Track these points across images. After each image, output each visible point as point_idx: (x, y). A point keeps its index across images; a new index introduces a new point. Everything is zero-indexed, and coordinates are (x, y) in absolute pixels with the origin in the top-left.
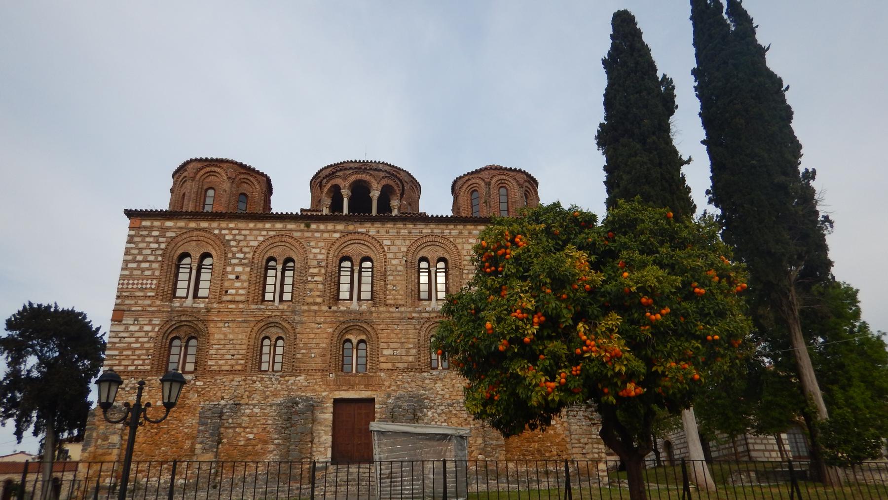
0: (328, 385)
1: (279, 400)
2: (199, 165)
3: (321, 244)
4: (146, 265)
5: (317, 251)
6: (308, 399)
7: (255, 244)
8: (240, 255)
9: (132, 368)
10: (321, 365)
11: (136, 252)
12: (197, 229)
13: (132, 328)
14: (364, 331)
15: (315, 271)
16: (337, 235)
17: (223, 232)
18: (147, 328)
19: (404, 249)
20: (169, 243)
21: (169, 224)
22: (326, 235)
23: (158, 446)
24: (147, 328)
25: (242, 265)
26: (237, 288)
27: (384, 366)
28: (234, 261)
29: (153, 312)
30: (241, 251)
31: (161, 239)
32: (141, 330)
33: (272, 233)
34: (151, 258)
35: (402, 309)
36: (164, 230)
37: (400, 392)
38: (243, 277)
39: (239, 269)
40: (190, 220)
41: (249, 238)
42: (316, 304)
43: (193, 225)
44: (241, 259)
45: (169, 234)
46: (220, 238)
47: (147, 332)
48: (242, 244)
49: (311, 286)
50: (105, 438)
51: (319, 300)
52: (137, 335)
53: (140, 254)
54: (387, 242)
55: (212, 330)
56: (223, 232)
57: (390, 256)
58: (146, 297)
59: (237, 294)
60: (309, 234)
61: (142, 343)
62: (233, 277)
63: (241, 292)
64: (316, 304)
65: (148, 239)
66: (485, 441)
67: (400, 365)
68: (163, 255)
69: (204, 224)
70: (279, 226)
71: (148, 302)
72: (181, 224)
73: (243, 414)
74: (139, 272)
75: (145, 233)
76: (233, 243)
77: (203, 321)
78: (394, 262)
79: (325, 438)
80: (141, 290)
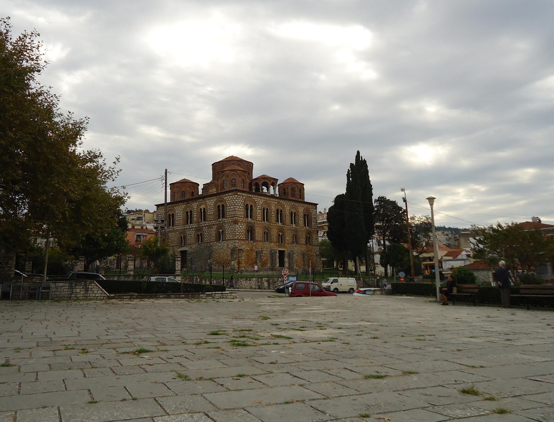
0: (277, 246)
1: (269, 250)
2: (242, 172)
3: (274, 205)
4: (240, 207)
5: (273, 207)
6: (274, 250)
7: (261, 203)
8: (259, 207)
9: (242, 238)
10: (276, 241)
11: (238, 202)
12: (249, 197)
13: (241, 227)
14: (282, 232)
15: (273, 213)
16: (276, 203)
17: (255, 198)
18: (243, 227)
19: (289, 209)
20: (244, 201)
21: (244, 194)
22: (274, 202)
23: (249, 260)
24: (243, 227)
25: (259, 210)
26: (259, 217)
27: (287, 242)
28: (258, 208)
29: (244, 222)
30: (259, 205)
31: (243, 199)
32: (242, 227)
33: (264, 200)
34: (241, 205)
35: (289, 226)
36: (243, 196)
37: (290, 249)
38: (260, 213)
39: (259, 211)
40: (248, 194)
41: (260, 201)
42: (274, 223)
43: (248, 195)
44: (259, 208)
45: (244, 198)
46: (254, 200)
47: (243, 228)
48: (259, 203)
49: (273, 218)
50: (241, 258)
51: (274, 222)
52: (242, 228)
53: (239, 203)
54: (286, 206)
55: (256, 229)
56: (255, 198)
57: (286, 210)
58: (242, 217)
59: (259, 219)
60: (271, 202)
61: (243, 231)
62: (258, 213)
63: (260, 218)
64: (274, 223)
65: (240, 199)
66: (304, 263)
67: (289, 242)
68: (244, 204)
69: (251, 196)
70: (265, 198)
71: (242, 219)
72: (246, 195)
73: (263, 253)
74: (239, 209)
75: (239, 197)
76: (257, 203)
77: (254, 226)
78: (287, 212)
79: (278, 260)
80: (241, 215)
